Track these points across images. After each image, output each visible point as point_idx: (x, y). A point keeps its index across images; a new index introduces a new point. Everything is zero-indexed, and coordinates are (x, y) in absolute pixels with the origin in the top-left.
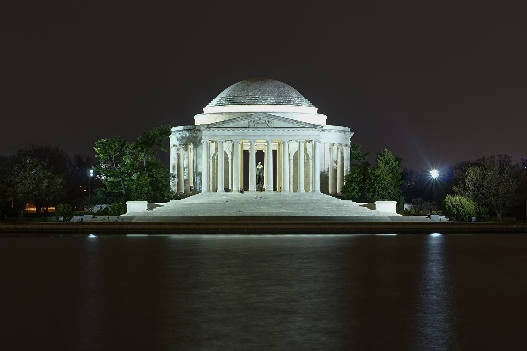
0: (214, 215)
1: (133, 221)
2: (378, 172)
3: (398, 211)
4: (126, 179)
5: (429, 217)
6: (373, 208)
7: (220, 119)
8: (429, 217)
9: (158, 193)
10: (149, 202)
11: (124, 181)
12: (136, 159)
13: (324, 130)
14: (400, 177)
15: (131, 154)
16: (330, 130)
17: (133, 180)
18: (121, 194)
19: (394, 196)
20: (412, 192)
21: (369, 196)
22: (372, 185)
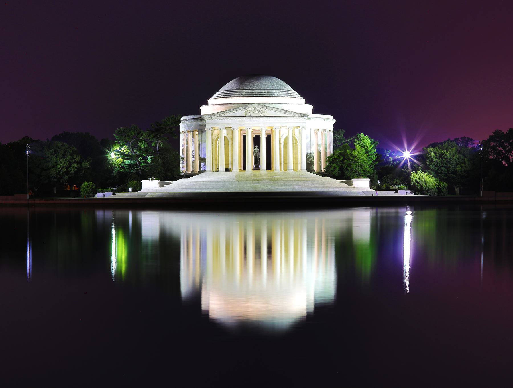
0: (215, 191)
1: (146, 197)
2: (355, 153)
3: (371, 187)
4: (142, 161)
5: (397, 192)
6: (350, 184)
7: (221, 109)
8: (397, 192)
9: (169, 172)
10: (161, 181)
11: (140, 163)
12: (149, 144)
13: (309, 118)
14: (374, 159)
15: (146, 141)
16: (314, 118)
17: (148, 162)
18: (137, 173)
19: (369, 174)
20: (384, 173)
21: (348, 174)
22: (349, 165)
